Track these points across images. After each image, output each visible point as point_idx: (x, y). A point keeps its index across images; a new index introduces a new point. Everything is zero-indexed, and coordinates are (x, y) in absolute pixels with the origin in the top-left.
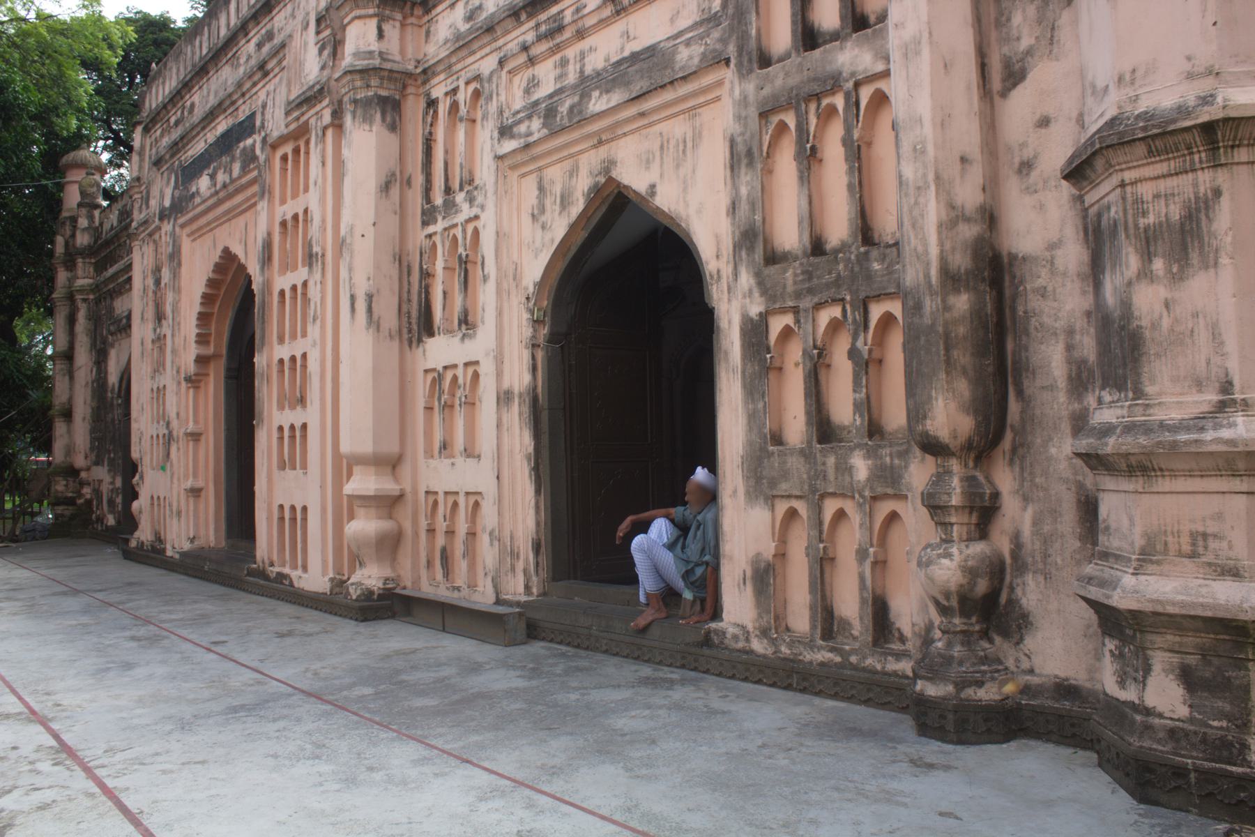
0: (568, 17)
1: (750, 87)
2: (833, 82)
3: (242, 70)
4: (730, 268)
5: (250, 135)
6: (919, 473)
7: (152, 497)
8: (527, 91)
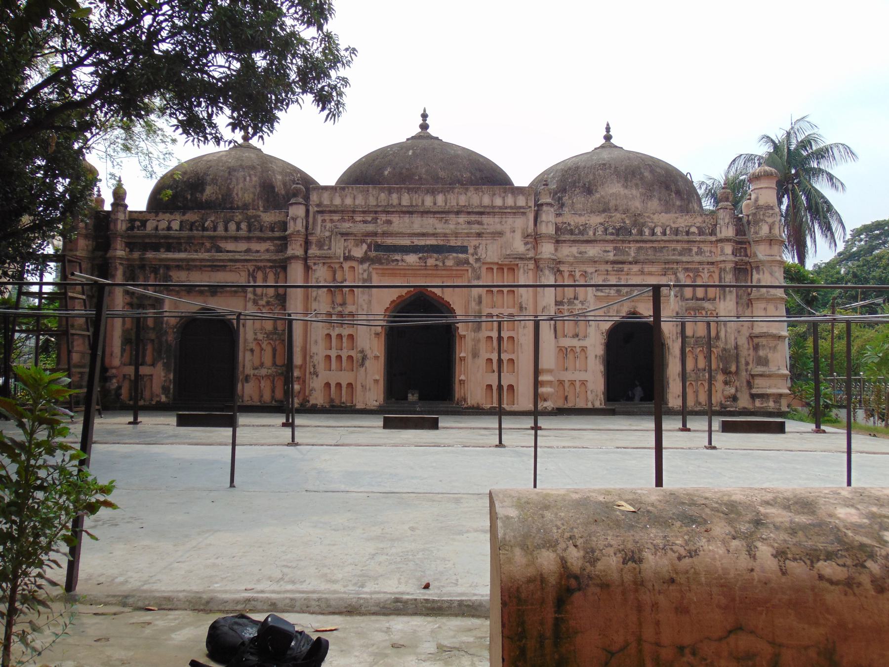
0: (625, 269)
1: (684, 304)
2: (704, 309)
3: (452, 227)
4: (674, 337)
5: (462, 253)
6: (720, 378)
7: (328, 385)
8: (604, 281)
